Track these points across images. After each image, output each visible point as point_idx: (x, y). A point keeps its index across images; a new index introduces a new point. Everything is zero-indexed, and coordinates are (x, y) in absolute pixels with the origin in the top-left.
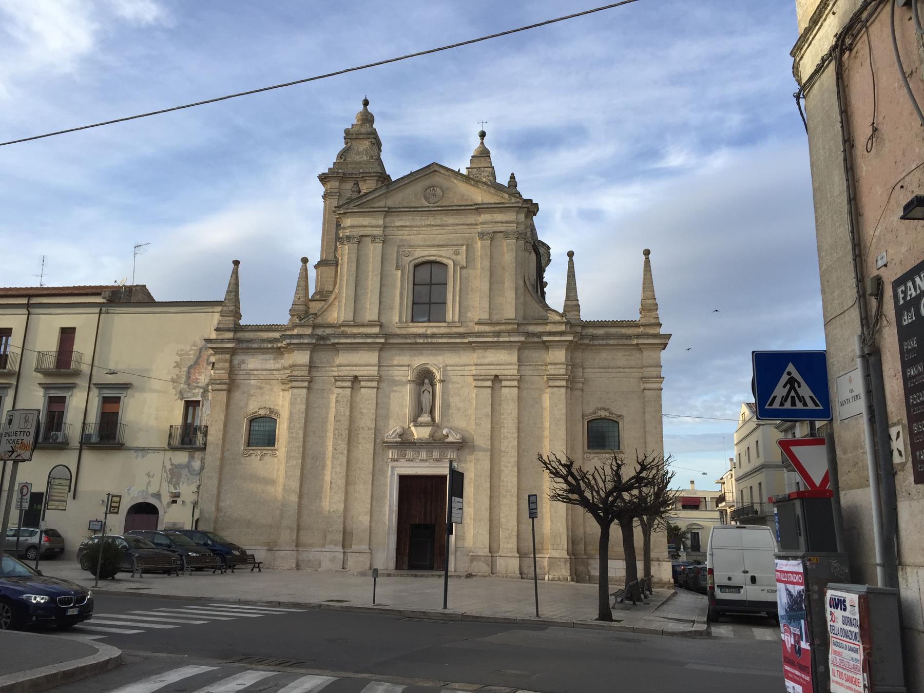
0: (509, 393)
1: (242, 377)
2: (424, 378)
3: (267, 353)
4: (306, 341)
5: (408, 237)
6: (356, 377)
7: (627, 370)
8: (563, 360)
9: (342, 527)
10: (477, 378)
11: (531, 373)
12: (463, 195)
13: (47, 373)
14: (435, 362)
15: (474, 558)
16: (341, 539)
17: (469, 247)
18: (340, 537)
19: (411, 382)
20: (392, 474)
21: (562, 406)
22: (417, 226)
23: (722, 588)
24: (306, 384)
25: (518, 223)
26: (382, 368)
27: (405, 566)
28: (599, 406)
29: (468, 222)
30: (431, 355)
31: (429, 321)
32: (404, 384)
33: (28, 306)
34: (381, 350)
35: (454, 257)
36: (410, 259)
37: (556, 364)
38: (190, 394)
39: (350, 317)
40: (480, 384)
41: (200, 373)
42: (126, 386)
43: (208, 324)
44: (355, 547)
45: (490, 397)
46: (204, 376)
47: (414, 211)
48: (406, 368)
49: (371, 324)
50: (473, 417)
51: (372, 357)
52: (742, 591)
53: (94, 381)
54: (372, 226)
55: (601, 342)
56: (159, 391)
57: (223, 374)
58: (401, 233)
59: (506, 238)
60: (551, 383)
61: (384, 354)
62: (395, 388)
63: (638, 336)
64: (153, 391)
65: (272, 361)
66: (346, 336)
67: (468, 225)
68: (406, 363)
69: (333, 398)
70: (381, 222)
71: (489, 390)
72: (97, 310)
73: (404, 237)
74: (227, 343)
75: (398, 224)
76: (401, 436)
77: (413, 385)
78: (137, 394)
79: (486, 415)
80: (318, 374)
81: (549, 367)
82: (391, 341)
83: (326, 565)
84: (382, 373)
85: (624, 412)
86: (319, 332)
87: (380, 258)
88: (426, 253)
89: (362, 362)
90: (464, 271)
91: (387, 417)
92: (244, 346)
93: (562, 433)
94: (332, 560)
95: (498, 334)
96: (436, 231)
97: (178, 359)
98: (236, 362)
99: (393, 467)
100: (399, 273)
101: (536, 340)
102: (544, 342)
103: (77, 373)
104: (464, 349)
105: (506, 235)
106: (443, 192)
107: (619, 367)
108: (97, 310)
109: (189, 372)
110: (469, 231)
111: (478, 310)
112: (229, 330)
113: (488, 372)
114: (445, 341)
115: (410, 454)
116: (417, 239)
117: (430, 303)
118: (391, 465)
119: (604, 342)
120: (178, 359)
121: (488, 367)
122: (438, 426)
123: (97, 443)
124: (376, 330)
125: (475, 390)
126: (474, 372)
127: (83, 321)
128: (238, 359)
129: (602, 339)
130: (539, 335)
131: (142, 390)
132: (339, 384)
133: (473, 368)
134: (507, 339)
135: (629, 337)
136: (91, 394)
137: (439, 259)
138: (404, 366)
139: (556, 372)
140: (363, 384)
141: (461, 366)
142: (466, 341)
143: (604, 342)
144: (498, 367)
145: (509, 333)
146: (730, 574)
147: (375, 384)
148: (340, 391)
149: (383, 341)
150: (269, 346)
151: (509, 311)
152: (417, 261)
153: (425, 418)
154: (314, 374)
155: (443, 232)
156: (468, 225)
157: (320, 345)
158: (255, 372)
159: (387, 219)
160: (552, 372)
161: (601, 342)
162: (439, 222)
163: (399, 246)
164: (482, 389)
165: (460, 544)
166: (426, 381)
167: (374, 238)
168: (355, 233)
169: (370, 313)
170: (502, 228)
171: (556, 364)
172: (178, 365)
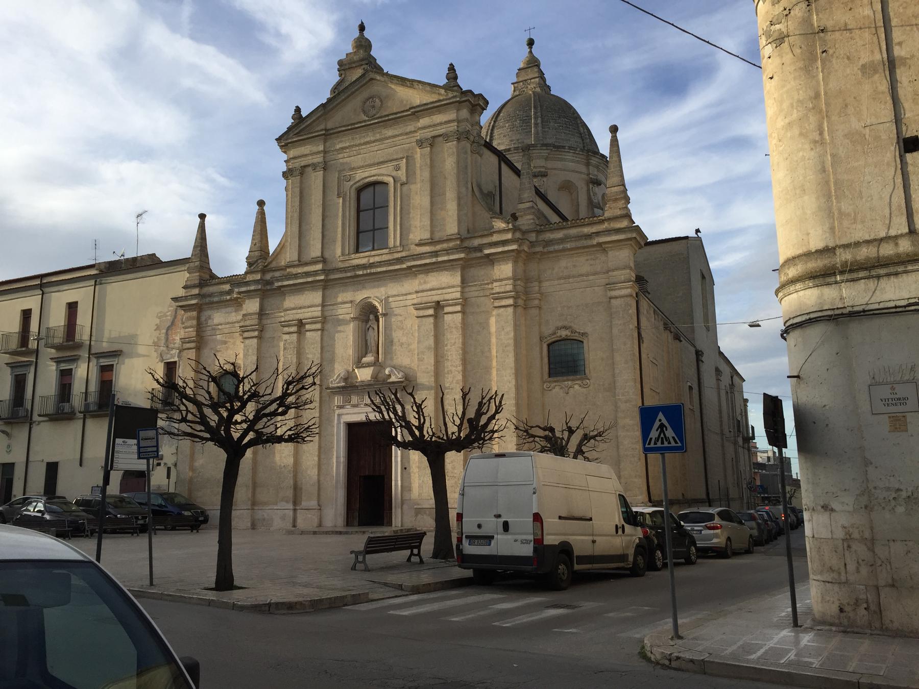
0: (452, 319)
1: (209, 333)
2: (368, 314)
3: (228, 306)
4: (252, 288)
5: (348, 160)
6: (300, 321)
7: (591, 278)
8: (510, 274)
9: (292, 482)
10: (418, 307)
11: (476, 294)
12: (402, 101)
13: (59, 348)
14: (375, 294)
15: (419, 511)
16: (291, 496)
17: (409, 159)
18: (290, 493)
19: (354, 319)
20: (339, 422)
21: (510, 328)
22: (356, 146)
23: (472, 538)
24: (256, 333)
25: (459, 121)
26: (326, 308)
27: (356, 523)
28: (560, 324)
29: (408, 130)
30: (374, 287)
31: (373, 249)
32: (345, 322)
33: (41, 286)
34: (325, 288)
35: (394, 173)
36: (352, 183)
37: (501, 280)
38: (169, 356)
39: (295, 257)
40: (422, 313)
41: (176, 333)
42: (116, 354)
43: (176, 283)
44: (304, 504)
45: (432, 326)
46: (177, 337)
47: (352, 128)
48: (350, 305)
49: (314, 262)
50: (416, 352)
51: (316, 297)
52: (493, 542)
53: (93, 351)
54: (312, 154)
55: (556, 247)
56: (144, 356)
57: (192, 332)
58: (340, 156)
59: (447, 141)
60: (497, 304)
61: (328, 292)
62: (339, 328)
63: (598, 234)
64: (139, 356)
65: (234, 314)
66: (296, 276)
67: (407, 134)
68: (349, 299)
69: (282, 344)
70: (321, 148)
71: (431, 320)
72: (92, 282)
73: (345, 160)
74: (192, 299)
75: (338, 147)
76: (346, 379)
77: (357, 322)
78: (127, 361)
79: (429, 348)
80: (269, 321)
81: (495, 284)
82: (332, 277)
83: (277, 523)
84: (326, 314)
85: (588, 329)
86: (268, 276)
87: (321, 187)
88: (366, 174)
89: (307, 303)
90: (405, 188)
91: (332, 361)
92: (207, 300)
93: (510, 360)
94: (283, 518)
95: (435, 254)
96: (375, 147)
97: (158, 321)
98: (203, 319)
99: (339, 415)
100: (341, 200)
101: (479, 254)
102: (488, 255)
103: (79, 346)
104: (406, 276)
105: (446, 137)
106: (381, 101)
107: (582, 275)
108: (92, 282)
109: (167, 334)
110: (408, 141)
111: (419, 230)
112: (194, 286)
113: (429, 299)
114: (384, 269)
115: (355, 399)
116: (357, 161)
117: (374, 230)
118: (337, 412)
119: (561, 247)
120: (158, 321)
121: (429, 293)
122: (381, 366)
123: (95, 411)
124: (319, 267)
125: (417, 320)
126: (415, 301)
127: (81, 294)
128: (206, 314)
129: (558, 244)
130: (480, 249)
131: (131, 355)
132: (286, 329)
133: (414, 296)
134: (445, 258)
135: (589, 236)
136: (91, 364)
137: (380, 178)
138: (347, 302)
139: (502, 290)
140: (308, 327)
141: (403, 295)
142: (404, 266)
143: (561, 247)
144: (439, 292)
145: (447, 251)
146: (480, 520)
147: (319, 326)
148: (286, 337)
149: (322, 277)
150: (228, 297)
151: (451, 227)
152: (358, 185)
153: (369, 358)
154: (265, 322)
155: (382, 146)
156: (407, 134)
157: (267, 290)
158: (220, 327)
159: (328, 144)
160: (497, 290)
161: (556, 247)
162: (378, 136)
163: (340, 172)
164: (424, 319)
165: (406, 497)
166: (372, 317)
167: (314, 166)
168: (297, 165)
169: (315, 251)
170: (441, 130)
171: (501, 280)
172: (158, 328)
